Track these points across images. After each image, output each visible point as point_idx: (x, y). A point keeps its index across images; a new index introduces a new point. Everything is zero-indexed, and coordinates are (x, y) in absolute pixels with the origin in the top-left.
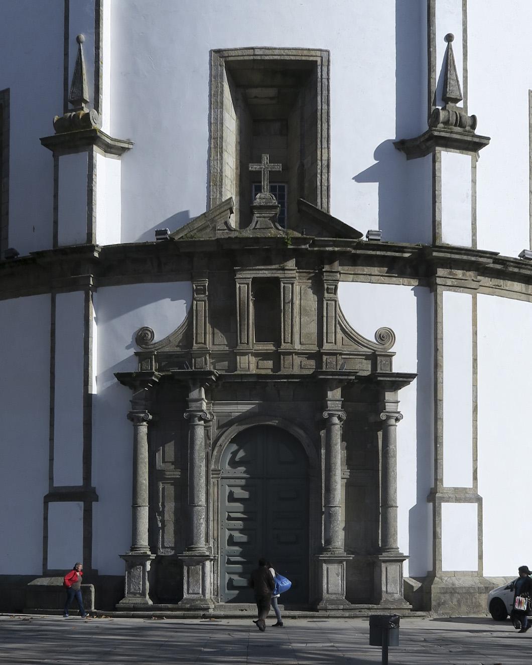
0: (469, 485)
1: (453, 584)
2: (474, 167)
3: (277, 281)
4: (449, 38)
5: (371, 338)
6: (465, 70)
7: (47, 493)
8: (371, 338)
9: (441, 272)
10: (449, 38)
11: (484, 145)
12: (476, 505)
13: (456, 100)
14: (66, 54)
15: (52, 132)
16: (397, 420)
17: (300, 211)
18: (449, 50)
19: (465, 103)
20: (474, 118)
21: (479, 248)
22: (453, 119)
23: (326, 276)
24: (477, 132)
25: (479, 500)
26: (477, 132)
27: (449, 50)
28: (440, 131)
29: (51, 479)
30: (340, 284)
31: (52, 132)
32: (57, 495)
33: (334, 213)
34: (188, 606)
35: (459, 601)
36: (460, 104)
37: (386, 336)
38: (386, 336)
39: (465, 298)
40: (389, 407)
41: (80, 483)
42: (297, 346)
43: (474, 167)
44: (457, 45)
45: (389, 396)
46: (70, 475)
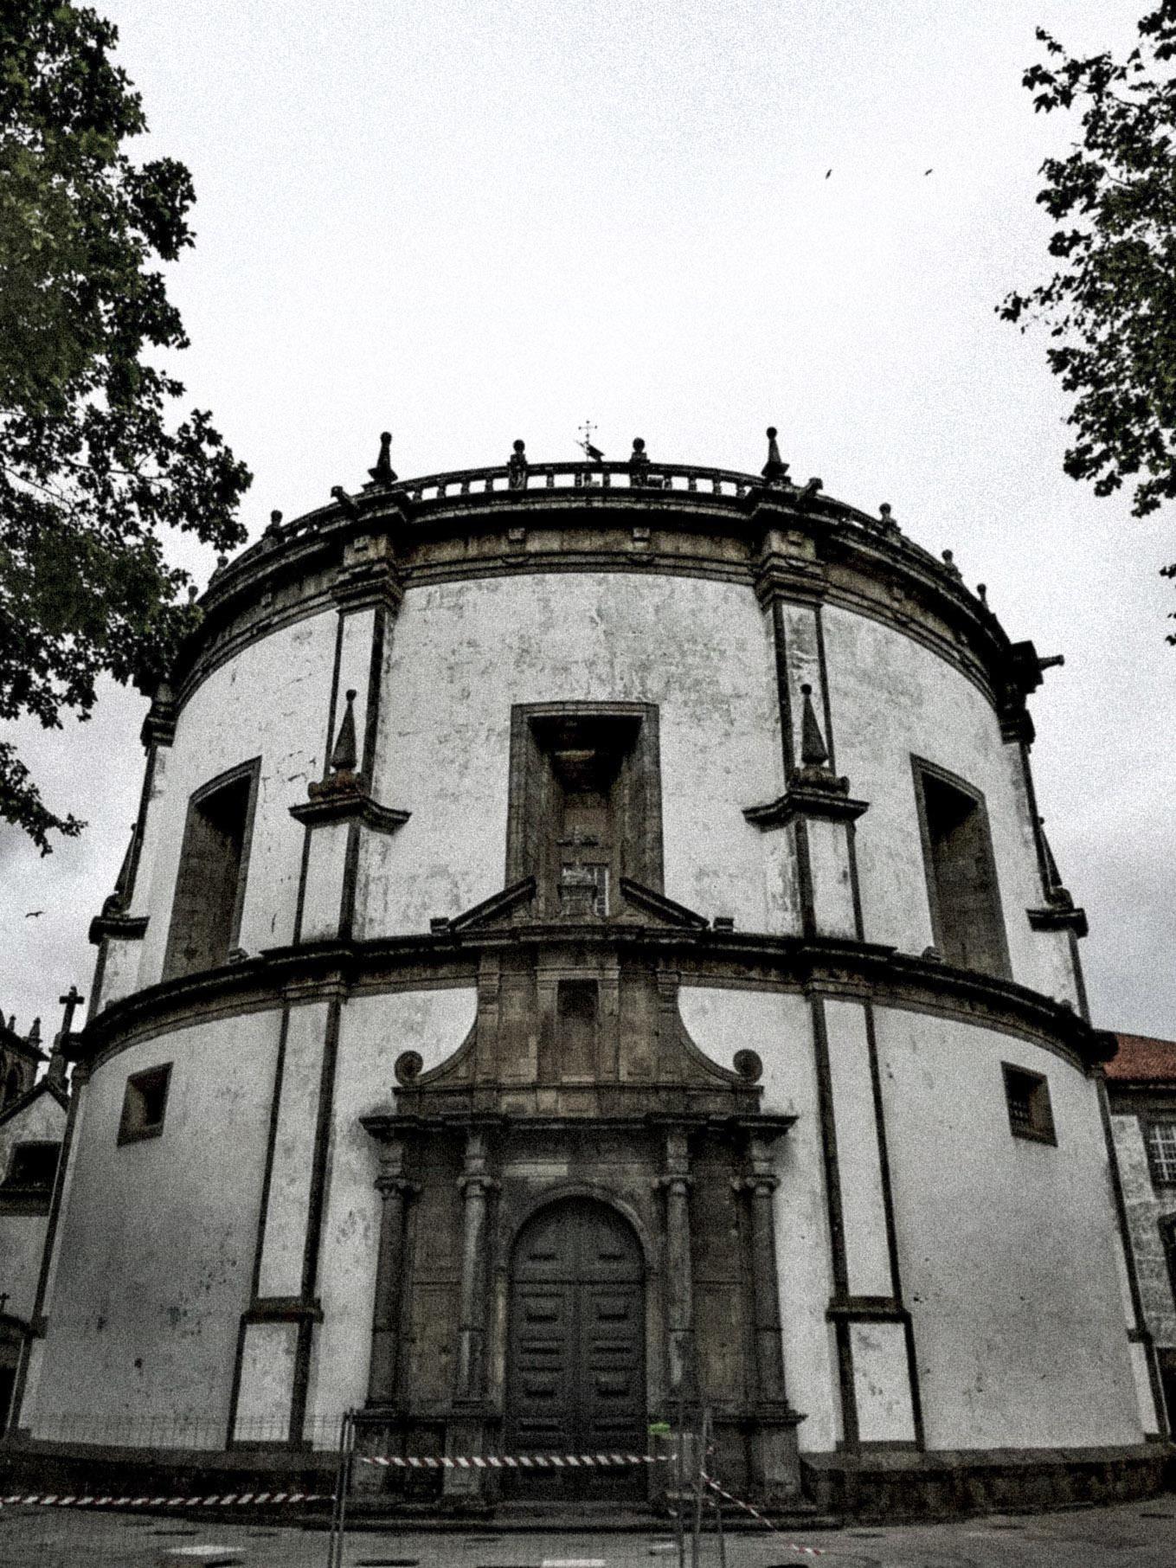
0: (890, 1293)
1: (879, 1465)
2: (851, 841)
3: (594, 982)
5: (729, 1065)
7: (246, 1307)
8: (729, 1065)
10: (806, 689)
11: (862, 812)
12: (900, 1329)
14: (333, 712)
15: (305, 799)
16: (772, 1188)
17: (624, 893)
18: (807, 703)
19: (832, 763)
20: (844, 780)
23: (661, 978)
25: (903, 1317)
26: (852, 796)
27: (807, 703)
29: (255, 1284)
30: (683, 990)
31: (305, 799)
32: (262, 1312)
33: (667, 896)
34: (450, 1509)
35: (891, 1497)
36: (826, 764)
37: (749, 1063)
38: (749, 1063)
39: (856, 1011)
40: (761, 1167)
41: (297, 1291)
42: (624, 1077)
43: (851, 841)
45: (756, 1151)
46: (282, 1278)
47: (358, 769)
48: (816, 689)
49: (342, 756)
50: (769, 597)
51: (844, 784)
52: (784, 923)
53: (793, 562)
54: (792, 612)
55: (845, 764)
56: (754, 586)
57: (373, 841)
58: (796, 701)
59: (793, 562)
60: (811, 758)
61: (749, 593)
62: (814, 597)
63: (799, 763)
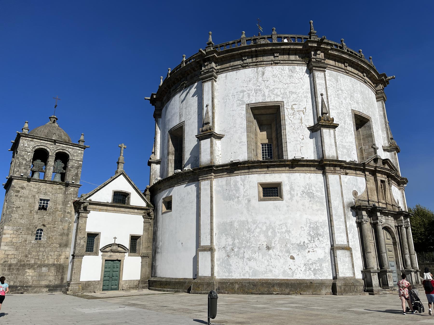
4: (322, 95)
9: (327, 168)
10: (322, 95)
13: (326, 114)
18: (322, 98)
19: (329, 114)
21: (340, 159)
22: (326, 119)
24: (334, 122)
26: (334, 122)
27: (322, 98)
28: (322, 122)
36: (328, 115)
39: (337, 176)
44: (324, 97)
48: (324, 93)
55: (333, 114)
60: (322, 114)
62: (323, 68)
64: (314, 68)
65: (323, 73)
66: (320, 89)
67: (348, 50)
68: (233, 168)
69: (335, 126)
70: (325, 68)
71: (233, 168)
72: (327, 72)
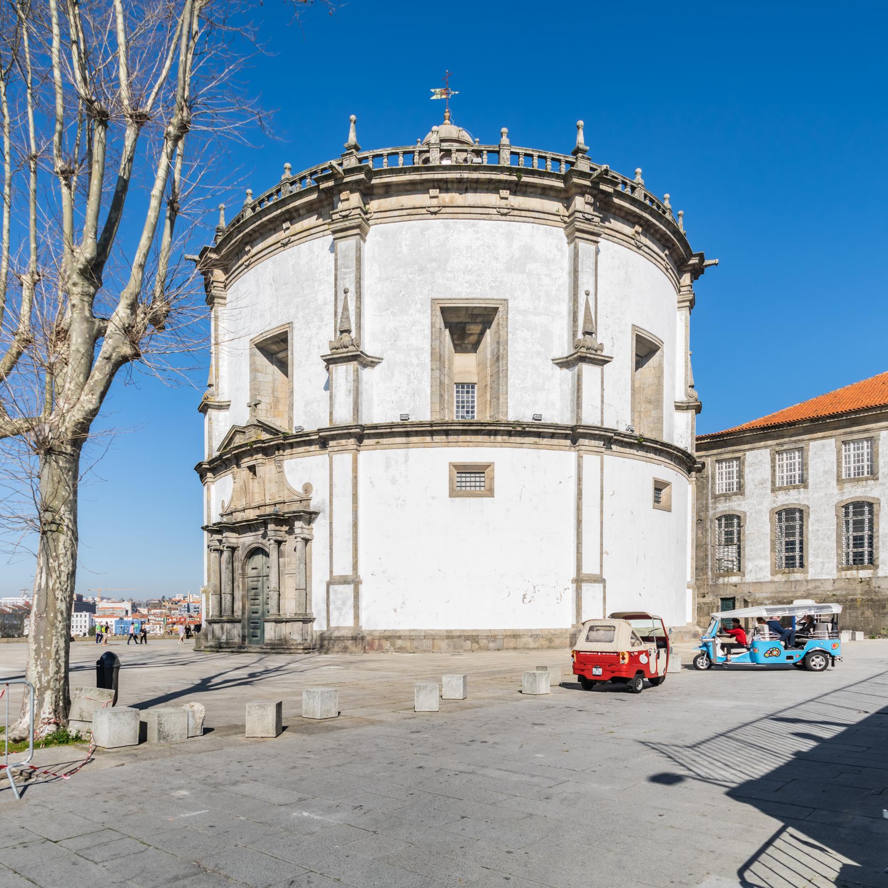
6: (596, 316)
18: (587, 301)
27: (587, 301)
47: (353, 334)
48: (592, 292)
49: (346, 327)
50: (571, 238)
51: (601, 347)
52: (566, 419)
53: (586, 215)
54: (582, 244)
55: (602, 337)
56: (565, 228)
57: (366, 373)
58: (582, 298)
59: (586, 215)
60: (586, 333)
61: (560, 233)
63: (580, 336)
64: (578, 234)
65: (592, 247)
66: (586, 282)
67: (646, 196)
68: (406, 431)
69: (603, 362)
70: (598, 235)
71: (406, 431)
72: (603, 243)
